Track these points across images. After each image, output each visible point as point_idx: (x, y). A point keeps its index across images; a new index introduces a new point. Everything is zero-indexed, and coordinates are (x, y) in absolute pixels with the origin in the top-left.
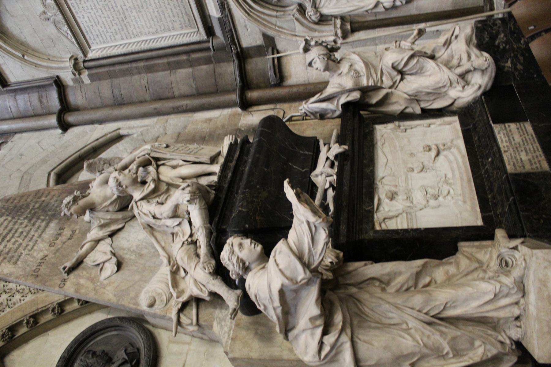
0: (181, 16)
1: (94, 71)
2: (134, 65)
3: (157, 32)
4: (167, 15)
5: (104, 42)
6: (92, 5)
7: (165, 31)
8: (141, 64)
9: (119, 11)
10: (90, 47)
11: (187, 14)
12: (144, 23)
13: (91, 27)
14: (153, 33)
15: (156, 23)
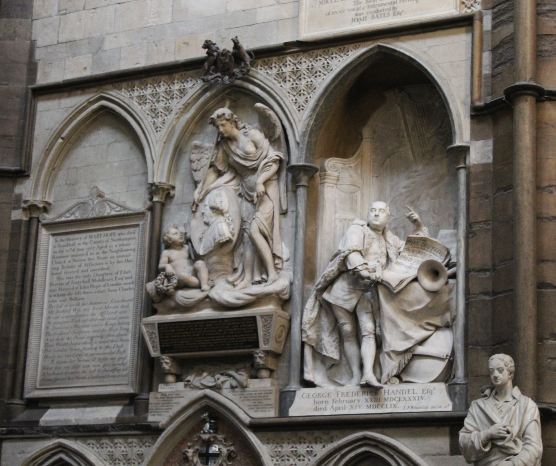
0: (56, 372)
1: (23, 229)
2: (17, 290)
3: (47, 334)
4: (61, 354)
5: (53, 257)
6: (93, 262)
7: (46, 345)
8: (16, 301)
9: (79, 293)
10: (53, 235)
11: (56, 380)
12: (60, 320)
13: (73, 248)
14: (47, 328)
15: (56, 337)
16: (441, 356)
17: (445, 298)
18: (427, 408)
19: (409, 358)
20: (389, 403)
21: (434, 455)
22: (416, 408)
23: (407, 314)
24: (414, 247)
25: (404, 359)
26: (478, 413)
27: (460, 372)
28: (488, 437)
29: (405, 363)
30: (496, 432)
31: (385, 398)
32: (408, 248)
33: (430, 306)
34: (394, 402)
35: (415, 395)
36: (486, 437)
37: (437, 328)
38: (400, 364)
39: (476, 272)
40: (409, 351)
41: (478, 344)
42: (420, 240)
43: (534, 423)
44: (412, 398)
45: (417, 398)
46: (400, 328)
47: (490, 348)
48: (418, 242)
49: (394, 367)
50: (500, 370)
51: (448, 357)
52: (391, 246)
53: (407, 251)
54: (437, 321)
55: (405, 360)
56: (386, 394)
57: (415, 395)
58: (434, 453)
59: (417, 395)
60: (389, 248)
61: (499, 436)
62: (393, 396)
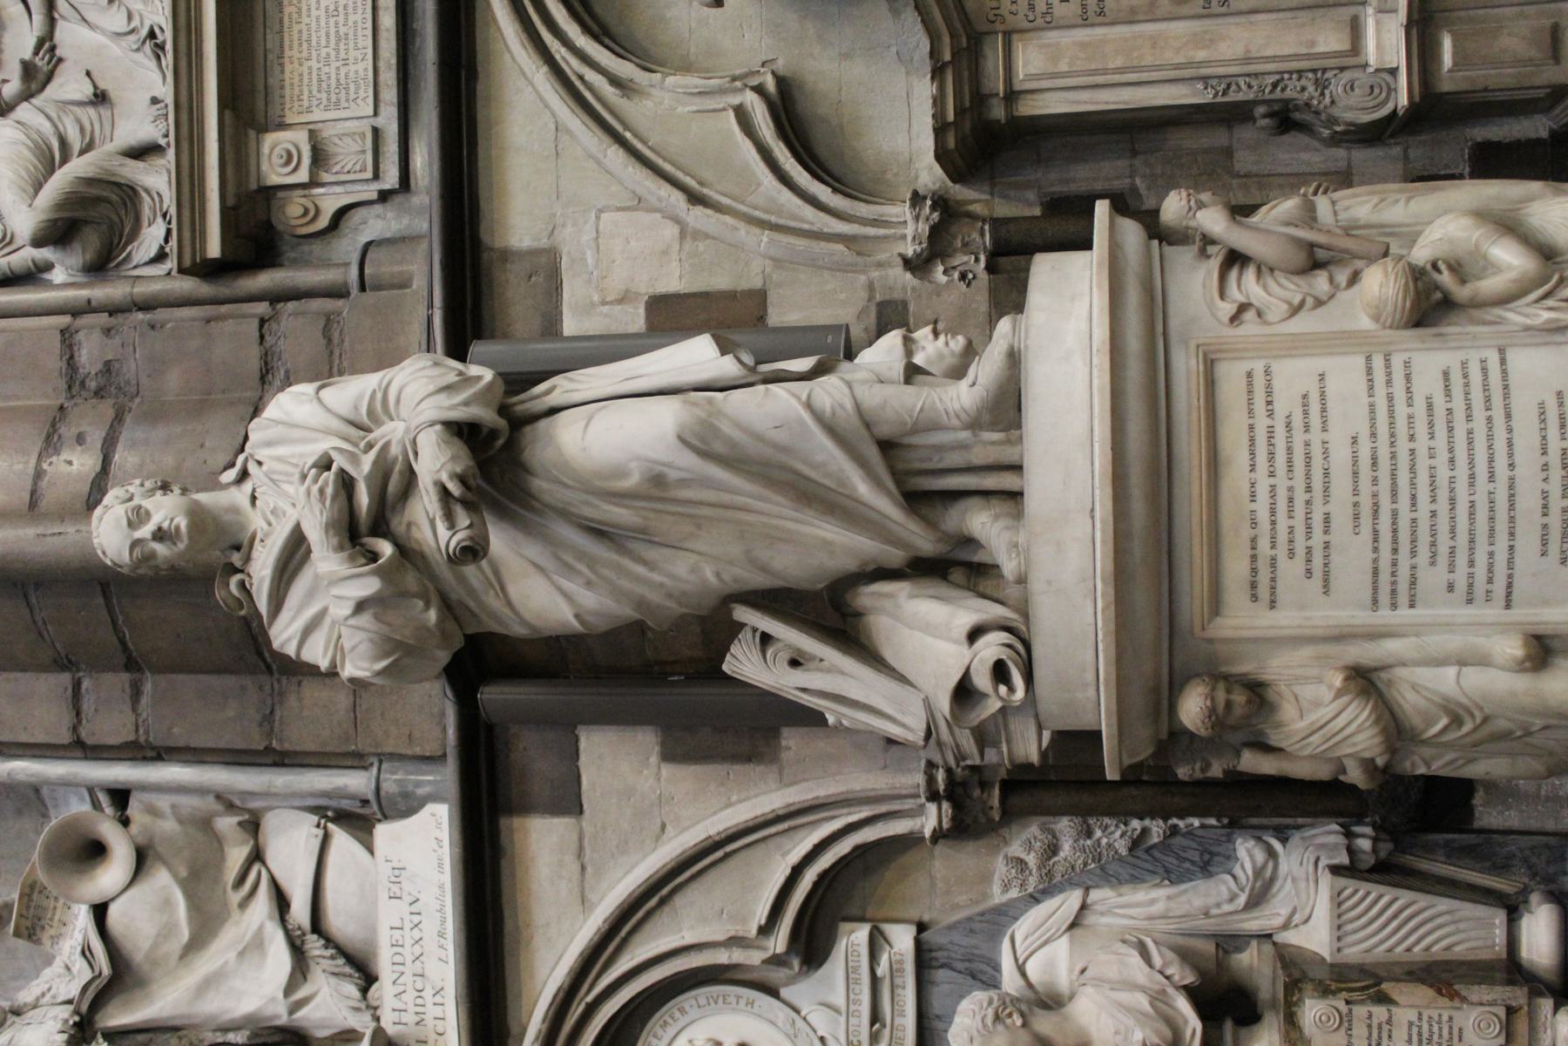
16: (315, 844)
17: (169, 826)
18: (441, 887)
19: (322, 942)
20: (432, 1012)
21: (583, 868)
22: (443, 922)
23: (196, 944)
24: (51, 919)
25: (321, 960)
26: (292, 613)
27: (356, 782)
28: (335, 541)
29: (332, 958)
30: (317, 507)
31: (417, 1024)
32: (52, 937)
33: (184, 873)
34: (428, 993)
35: (408, 926)
36: (340, 548)
37: (257, 856)
38: (334, 974)
39: (80, 722)
40: (298, 942)
41: (268, 718)
42: (30, 900)
43: (324, 393)
44: (416, 934)
45: (416, 919)
46: (226, 963)
47: (279, 681)
48: (38, 907)
49: (336, 990)
50: (138, 517)
51: (323, 821)
52: (49, 990)
53: (61, 943)
54: (237, 855)
55: (324, 957)
56: (406, 1018)
57: (408, 926)
58: (576, 867)
59: (407, 918)
60: (54, 997)
61: (335, 497)
62: (410, 997)
